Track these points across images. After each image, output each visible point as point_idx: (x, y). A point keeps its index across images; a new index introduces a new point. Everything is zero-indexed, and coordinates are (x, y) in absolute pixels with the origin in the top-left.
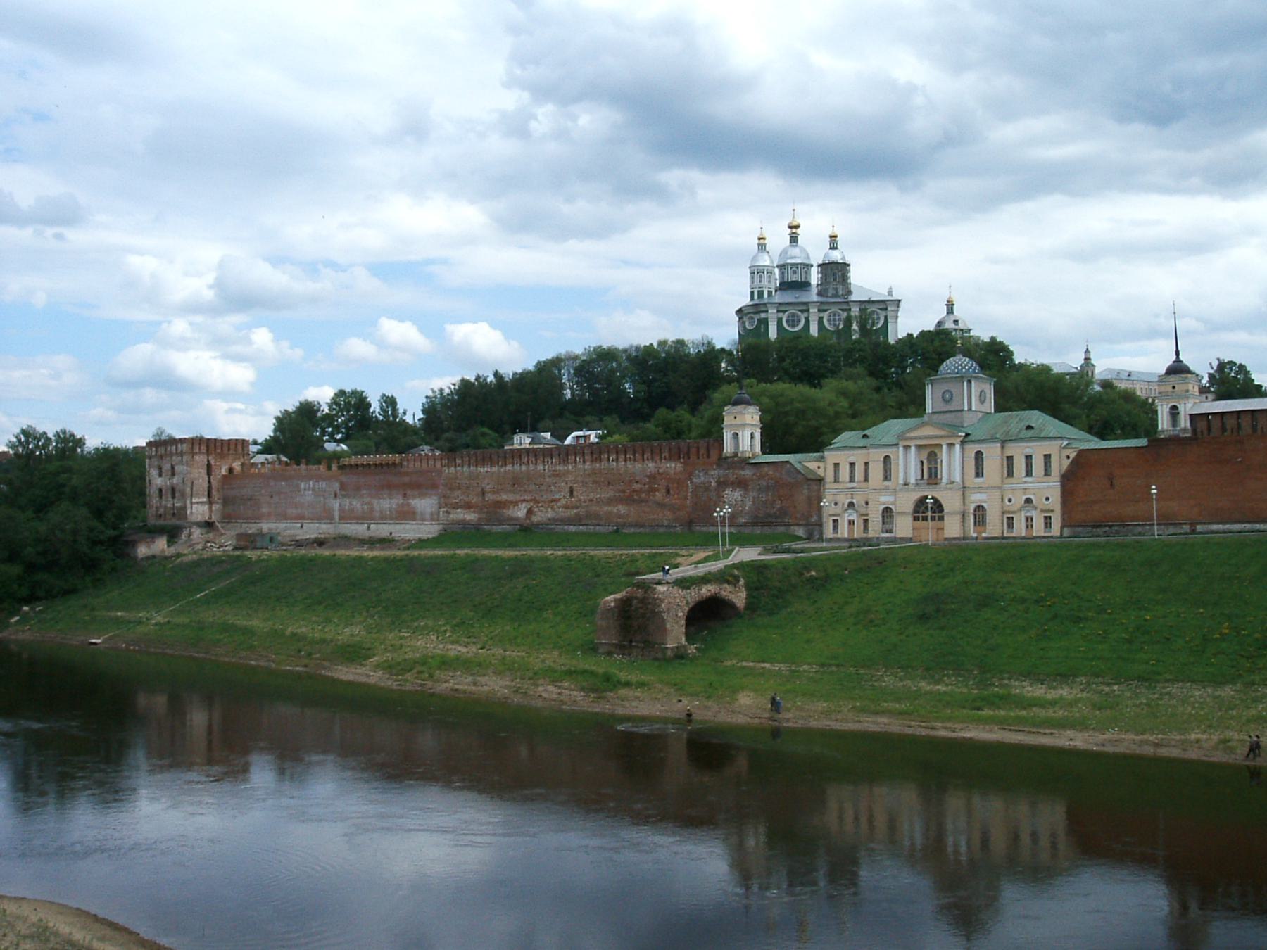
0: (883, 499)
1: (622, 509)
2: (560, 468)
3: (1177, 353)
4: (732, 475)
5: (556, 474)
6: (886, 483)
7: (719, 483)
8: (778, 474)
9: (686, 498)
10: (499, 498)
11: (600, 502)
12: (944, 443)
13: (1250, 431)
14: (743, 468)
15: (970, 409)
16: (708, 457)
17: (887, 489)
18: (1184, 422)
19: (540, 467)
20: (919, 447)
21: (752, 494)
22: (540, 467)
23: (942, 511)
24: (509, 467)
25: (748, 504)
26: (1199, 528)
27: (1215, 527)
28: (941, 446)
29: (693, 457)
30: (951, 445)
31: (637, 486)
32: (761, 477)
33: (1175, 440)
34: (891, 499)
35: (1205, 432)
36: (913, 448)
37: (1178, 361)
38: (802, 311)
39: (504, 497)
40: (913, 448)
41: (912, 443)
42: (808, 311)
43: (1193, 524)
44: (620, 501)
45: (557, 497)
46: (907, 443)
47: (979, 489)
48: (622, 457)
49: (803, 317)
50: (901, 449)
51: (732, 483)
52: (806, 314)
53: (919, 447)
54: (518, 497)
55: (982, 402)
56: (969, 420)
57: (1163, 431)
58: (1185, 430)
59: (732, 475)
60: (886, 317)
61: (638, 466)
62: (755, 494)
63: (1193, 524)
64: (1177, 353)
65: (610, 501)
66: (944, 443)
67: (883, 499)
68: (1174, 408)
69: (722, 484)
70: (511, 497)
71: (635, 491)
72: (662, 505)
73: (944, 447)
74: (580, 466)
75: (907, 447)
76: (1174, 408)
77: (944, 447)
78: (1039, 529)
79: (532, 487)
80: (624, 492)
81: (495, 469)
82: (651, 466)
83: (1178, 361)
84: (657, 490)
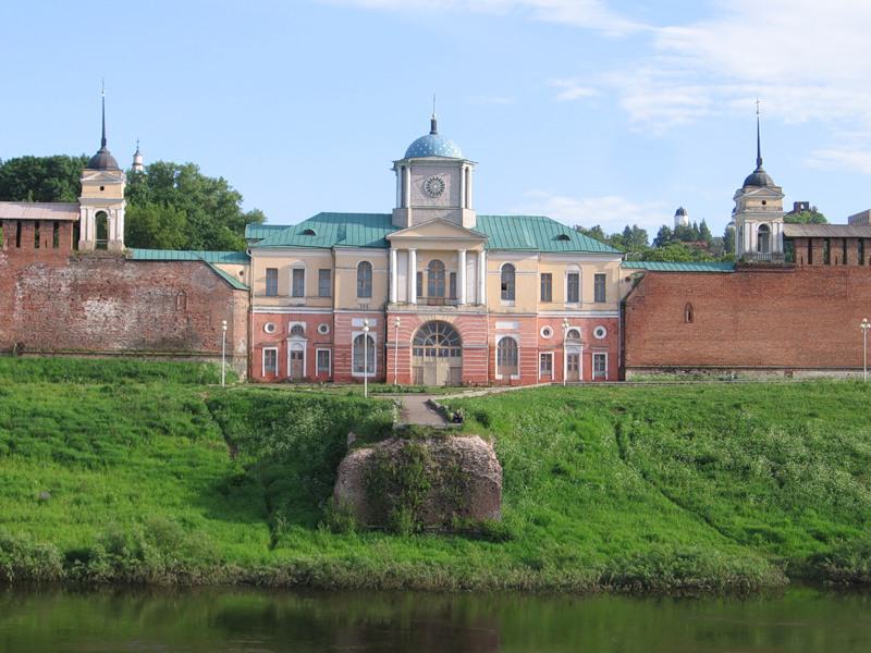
0: (356, 322)
4: (98, 276)
6: (363, 301)
7: (74, 286)
8: (182, 280)
9: (12, 308)
13: (856, 263)
16: (56, 244)
18: (776, 246)
23: (459, 343)
25: (129, 321)
28: (456, 253)
32: (154, 282)
35: (806, 260)
36: (414, 254)
47: (508, 316)
53: (418, 252)
57: (751, 254)
58: (777, 255)
62: (142, 307)
67: (356, 322)
69: (82, 290)
75: (404, 252)
76: (763, 227)
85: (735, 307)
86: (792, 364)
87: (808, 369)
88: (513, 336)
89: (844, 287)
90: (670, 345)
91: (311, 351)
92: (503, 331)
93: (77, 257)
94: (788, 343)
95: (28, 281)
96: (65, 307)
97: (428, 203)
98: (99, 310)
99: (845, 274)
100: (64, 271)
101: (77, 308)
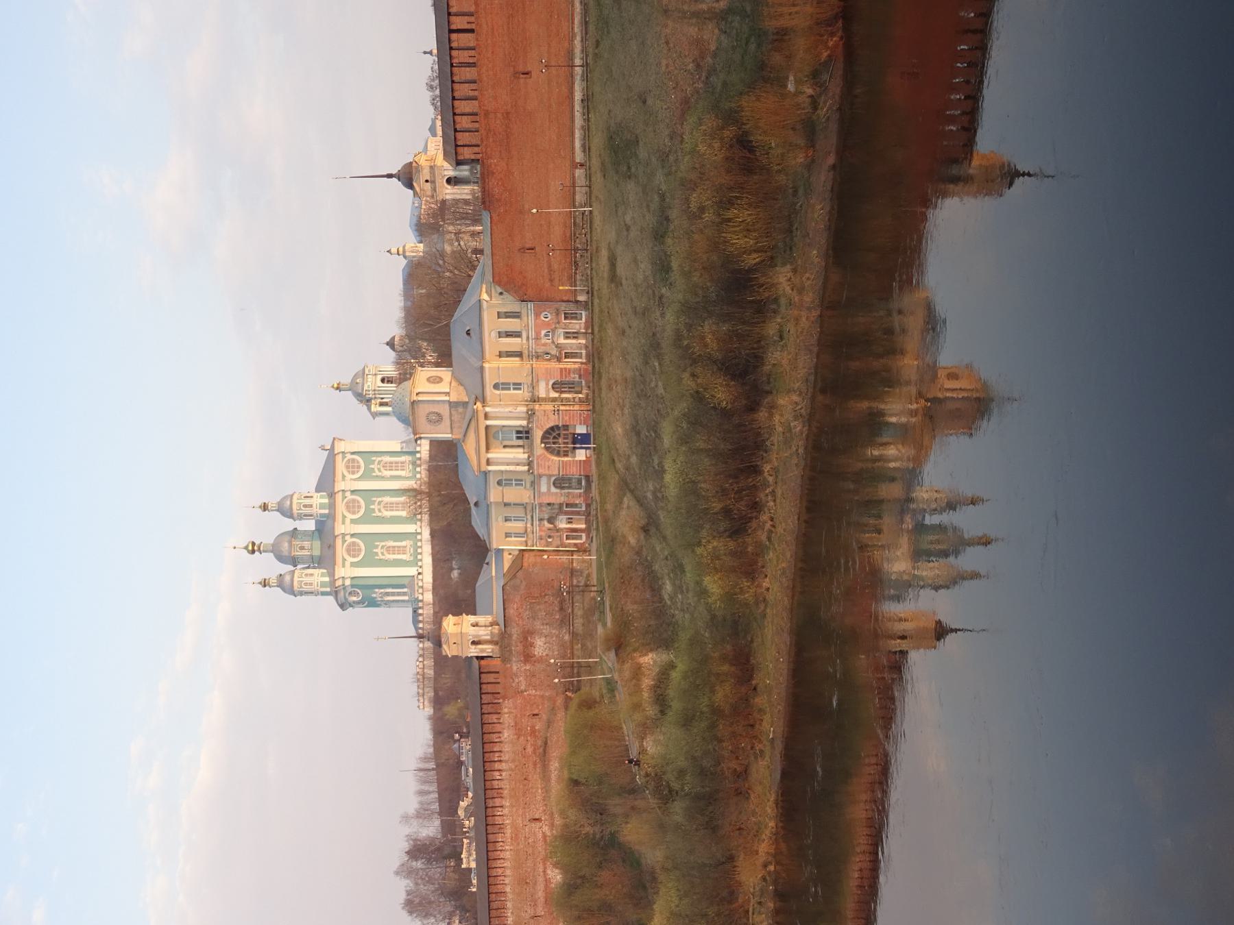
1: (554, 765)
2: (508, 831)
3: (390, 176)
4: (516, 647)
5: (515, 838)
9: (542, 697)
10: (542, 900)
11: (547, 790)
12: (484, 423)
14: (510, 636)
15: (447, 394)
17: (533, 483)
18: (464, 171)
19: (507, 855)
20: (488, 449)
21: (538, 625)
22: (507, 855)
23: (557, 427)
24: (508, 889)
25: (546, 630)
26: (579, 157)
27: (578, 144)
29: (498, 689)
30: (486, 416)
31: (530, 750)
33: (483, 180)
34: (544, 481)
35: (476, 150)
37: (397, 176)
38: (344, 541)
39: (540, 894)
40: (490, 455)
41: (485, 456)
42: (344, 535)
43: (575, 165)
44: (545, 767)
45: (540, 836)
46: (484, 462)
47: (533, 387)
48: (497, 766)
49: (349, 539)
50: (490, 468)
51: (525, 647)
52: (348, 538)
54: (541, 879)
55: (440, 380)
56: (458, 395)
59: (516, 647)
60: (353, 453)
61: (507, 748)
63: (575, 165)
64: (390, 176)
65: (545, 777)
66: (484, 423)
67: (544, 489)
68: (449, 181)
69: (528, 657)
70: (541, 887)
71: (534, 752)
72: (549, 723)
73: (489, 422)
74: (506, 811)
75: (488, 462)
76: (449, 181)
77: (489, 422)
78: (579, 325)
79: (530, 863)
80: (535, 764)
81: (509, 905)
82: (507, 735)
83: (397, 176)
84: (533, 727)
85: (521, 212)
86: (568, 163)
87: (573, 148)
88: (551, 383)
89: (499, 115)
90: (555, 266)
91: (566, 513)
92: (548, 391)
93: (505, 659)
94: (551, 166)
95: (523, 688)
96: (540, 667)
97: (447, 422)
98: (540, 646)
99: (487, 114)
100: (515, 668)
101: (541, 660)
